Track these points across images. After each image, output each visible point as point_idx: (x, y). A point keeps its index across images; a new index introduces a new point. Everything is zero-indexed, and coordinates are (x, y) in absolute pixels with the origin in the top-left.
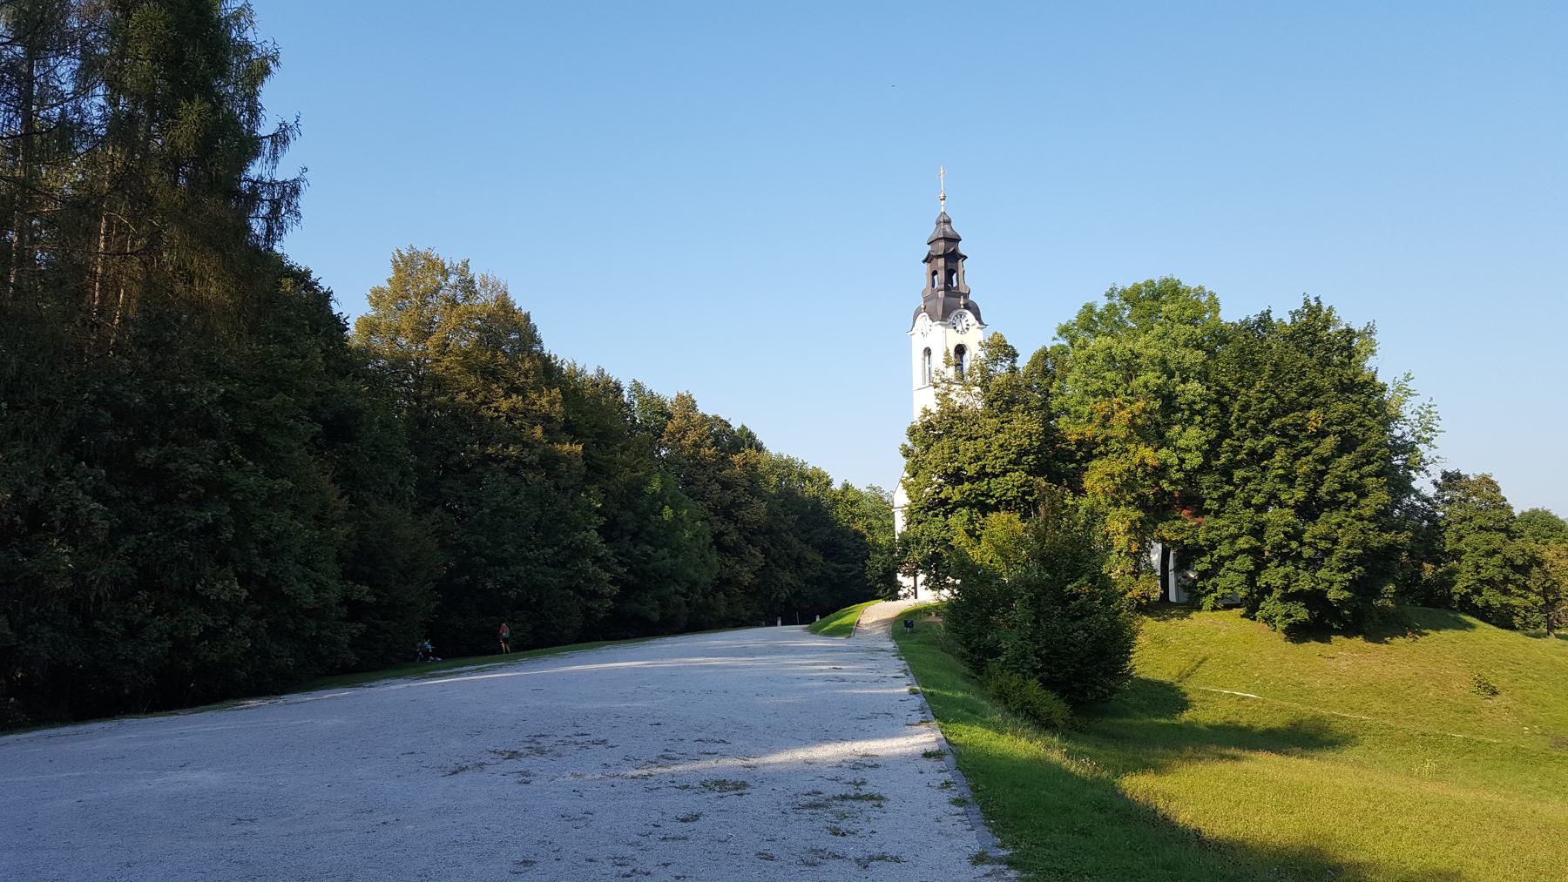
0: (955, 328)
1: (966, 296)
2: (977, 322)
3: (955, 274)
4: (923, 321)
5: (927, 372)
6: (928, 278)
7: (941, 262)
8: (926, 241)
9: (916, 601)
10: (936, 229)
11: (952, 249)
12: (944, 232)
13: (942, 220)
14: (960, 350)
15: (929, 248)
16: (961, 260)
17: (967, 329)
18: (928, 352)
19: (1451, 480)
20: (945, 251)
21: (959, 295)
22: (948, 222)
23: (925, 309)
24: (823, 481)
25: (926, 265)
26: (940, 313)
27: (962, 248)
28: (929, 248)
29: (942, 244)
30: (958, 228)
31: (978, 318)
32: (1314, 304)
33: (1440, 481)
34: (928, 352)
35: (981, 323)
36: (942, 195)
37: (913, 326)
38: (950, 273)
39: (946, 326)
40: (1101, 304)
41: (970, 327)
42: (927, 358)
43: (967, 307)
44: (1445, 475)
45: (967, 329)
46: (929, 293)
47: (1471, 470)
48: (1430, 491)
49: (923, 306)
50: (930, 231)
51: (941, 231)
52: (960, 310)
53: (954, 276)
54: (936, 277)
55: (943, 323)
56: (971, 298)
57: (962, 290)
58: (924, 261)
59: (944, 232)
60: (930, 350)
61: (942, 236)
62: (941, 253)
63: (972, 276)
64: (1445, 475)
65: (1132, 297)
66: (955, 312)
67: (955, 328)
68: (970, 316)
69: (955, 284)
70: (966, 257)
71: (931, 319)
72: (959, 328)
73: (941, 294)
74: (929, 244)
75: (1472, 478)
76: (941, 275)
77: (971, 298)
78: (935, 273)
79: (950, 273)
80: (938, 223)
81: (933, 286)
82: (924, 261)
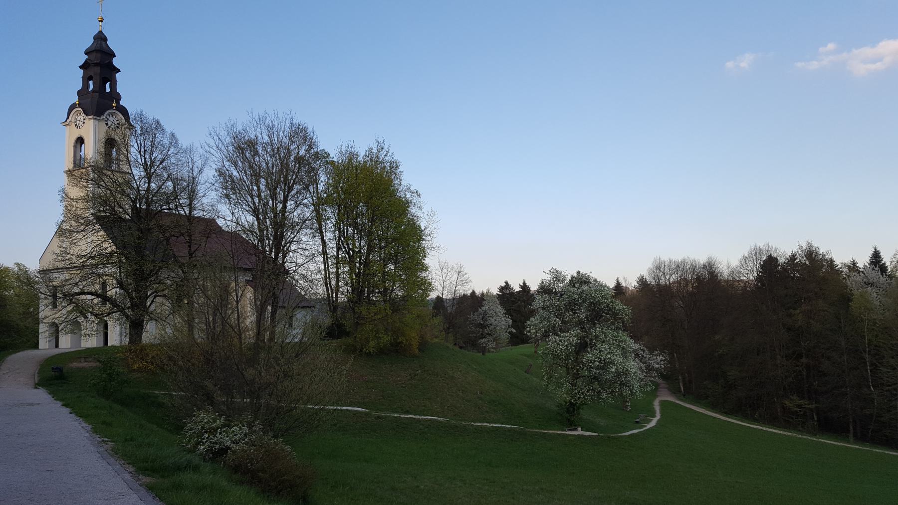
0: (107, 124)
3: (109, 83)
5: (78, 158)
9: (57, 349)
11: (107, 62)
15: (87, 57)
18: (80, 141)
22: (105, 39)
25: (82, 71)
27: (116, 62)
28: (87, 57)
29: (99, 55)
32: (380, 140)
34: (80, 141)
37: (68, 118)
42: (79, 146)
49: (77, 103)
50: (89, 42)
51: (98, 45)
53: (108, 85)
54: (91, 82)
55: (96, 117)
56: (122, 103)
58: (81, 67)
62: (98, 62)
63: (124, 85)
67: (107, 124)
69: (108, 90)
70: (120, 71)
74: (86, 53)
77: (122, 103)
78: (90, 78)
82: (81, 67)
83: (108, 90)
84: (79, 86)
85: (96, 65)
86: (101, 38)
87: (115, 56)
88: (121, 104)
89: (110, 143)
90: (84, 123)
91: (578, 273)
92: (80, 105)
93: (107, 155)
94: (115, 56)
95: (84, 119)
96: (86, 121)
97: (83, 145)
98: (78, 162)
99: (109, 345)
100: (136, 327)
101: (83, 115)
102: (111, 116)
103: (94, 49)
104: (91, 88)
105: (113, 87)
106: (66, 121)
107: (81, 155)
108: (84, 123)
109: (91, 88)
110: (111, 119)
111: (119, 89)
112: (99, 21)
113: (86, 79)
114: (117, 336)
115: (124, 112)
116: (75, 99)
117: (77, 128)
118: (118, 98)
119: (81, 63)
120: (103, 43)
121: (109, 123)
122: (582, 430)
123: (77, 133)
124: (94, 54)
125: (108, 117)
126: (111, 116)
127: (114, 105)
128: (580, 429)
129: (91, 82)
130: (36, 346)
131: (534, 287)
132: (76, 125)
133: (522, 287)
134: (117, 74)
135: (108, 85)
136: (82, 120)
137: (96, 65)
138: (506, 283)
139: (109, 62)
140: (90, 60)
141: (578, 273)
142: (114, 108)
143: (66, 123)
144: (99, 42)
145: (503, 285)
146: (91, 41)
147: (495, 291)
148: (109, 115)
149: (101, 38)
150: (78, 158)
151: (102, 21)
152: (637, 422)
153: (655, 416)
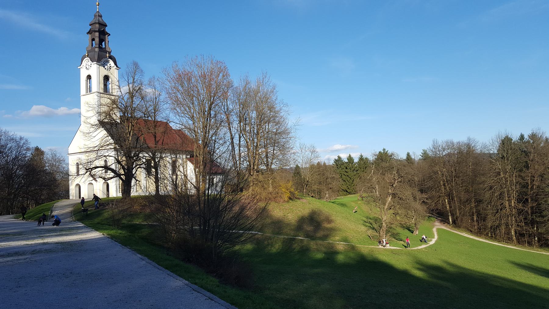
0: (104, 67)
1: (110, 53)
2: (115, 66)
3: (104, 42)
4: (87, 61)
5: (88, 87)
6: (89, 41)
7: (97, 34)
10: (94, 18)
11: (102, 29)
12: (99, 21)
13: (97, 15)
14: (106, 78)
15: (91, 27)
16: (107, 36)
18: (89, 77)
20: (99, 29)
21: (106, 52)
22: (101, 16)
23: (88, 56)
25: (89, 36)
26: (96, 58)
27: (107, 30)
29: (97, 26)
30: (105, 20)
31: (116, 64)
34: (89, 77)
35: (117, 66)
36: (97, 3)
37: (81, 64)
38: (101, 41)
39: (100, 65)
41: (112, 68)
42: (89, 80)
45: (111, 69)
46: (90, 49)
49: (87, 54)
50: (91, 19)
51: (97, 20)
52: (106, 59)
53: (103, 43)
54: (94, 42)
56: (112, 54)
57: (107, 50)
58: (88, 33)
59: (99, 21)
60: (90, 76)
61: (98, 22)
62: (98, 30)
68: (111, 63)
69: (104, 46)
72: (106, 67)
73: (97, 50)
74: (90, 25)
76: (97, 40)
77: (112, 54)
79: (101, 41)
80: (95, 16)
81: (92, 46)
82: (88, 33)
85: (95, 31)
88: (111, 54)
89: (106, 78)
91: (384, 150)
93: (105, 85)
95: (91, 64)
99: (110, 197)
100: (126, 187)
101: (91, 62)
102: (106, 62)
108: (91, 66)
112: (97, 5)
114: (115, 191)
117: (87, 69)
119: (88, 31)
120: (100, 18)
122: (390, 246)
125: (104, 62)
126: (106, 62)
127: (107, 55)
131: (356, 160)
132: (86, 68)
133: (348, 159)
136: (90, 65)
139: (104, 29)
140: (93, 29)
141: (384, 150)
142: (108, 57)
144: (98, 18)
145: (337, 158)
147: (332, 162)
148: (104, 62)
151: (98, 5)
153: (434, 238)
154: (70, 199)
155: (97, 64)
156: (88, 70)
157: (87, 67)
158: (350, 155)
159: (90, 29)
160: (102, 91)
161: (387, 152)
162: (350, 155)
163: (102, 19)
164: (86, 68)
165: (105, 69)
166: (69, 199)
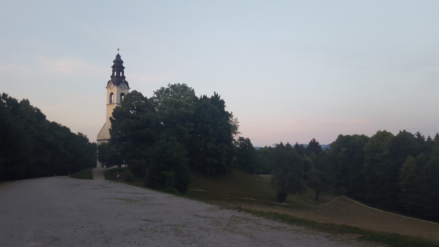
0: (121, 88)
1: (124, 80)
2: (128, 88)
8: (113, 61)
15: (113, 63)
17: (125, 89)
18: (112, 94)
19: (241, 139)
22: (120, 57)
23: (112, 81)
24: (66, 130)
25: (112, 68)
27: (124, 65)
28: (113, 63)
33: (239, 139)
34: (112, 94)
40: (166, 87)
43: (124, 83)
44: (240, 137)
47: (245, 138)
48: (237, 140)
49: (111, 80)
50: (115, 58)
53: (121, 73)
56: (126, 80)
58: (112, 67)
64: (240, 137)
65: (173, 87)
66: (122, 83)
69: (121, 75)
70: (125, 68)
71: (114, 84)
74: (113, 62)
75: (245, 138)
77: (126, 80)
81: (114, 74)
82: (112, 67)
83: (121, 75)
84: (111, 74)
86: (118, 56)
87: (123, 63)
90: (113, 88)
91: (314, 139)
92: (112, 81)
94: (123, 63)
96: (114, 87)
97: (113, 95)
98: (111, 102)
103: (116, 61)
104: (115, 75)
105: (123, 74)
106: (107, 87)
107: (112, 99)
108: (113, 88)
109: (115, 75)
110: (123, 86)
111: (125, 75)
113: (113, 72)
115: (127, 83)
116: (110, 79)
118: (124, 77)
119: (112, 65)
121: (122, 88)
122: (285, 203)
123: (110, 91)
124: (116, 63)
128: (284, 203)
129: (115, 72)
130: (95, 166)
132: (110, 88)
134: (124, 69)
135: (121, 73)
137: (117, 66)
138: (281, 143)
141: (314, 139)
143: (107, 87)
145: (280, 144)
146: (115, 57)
148: (122, 85)
149: (118, 56)
150: (111, 100)
151: (118, 50)
152: (316, 204)
154: (97, 167)
155: (117, 86)
156: (111, 90)
157: (112, 88)
158: (288, 143)
159: (114, 65)
160: (119, 103)
161: (315, 140)
162: (288, 143)
163: (121, 59)
164: (110, 88)
165: (122, 89)
166: (96, 167)
